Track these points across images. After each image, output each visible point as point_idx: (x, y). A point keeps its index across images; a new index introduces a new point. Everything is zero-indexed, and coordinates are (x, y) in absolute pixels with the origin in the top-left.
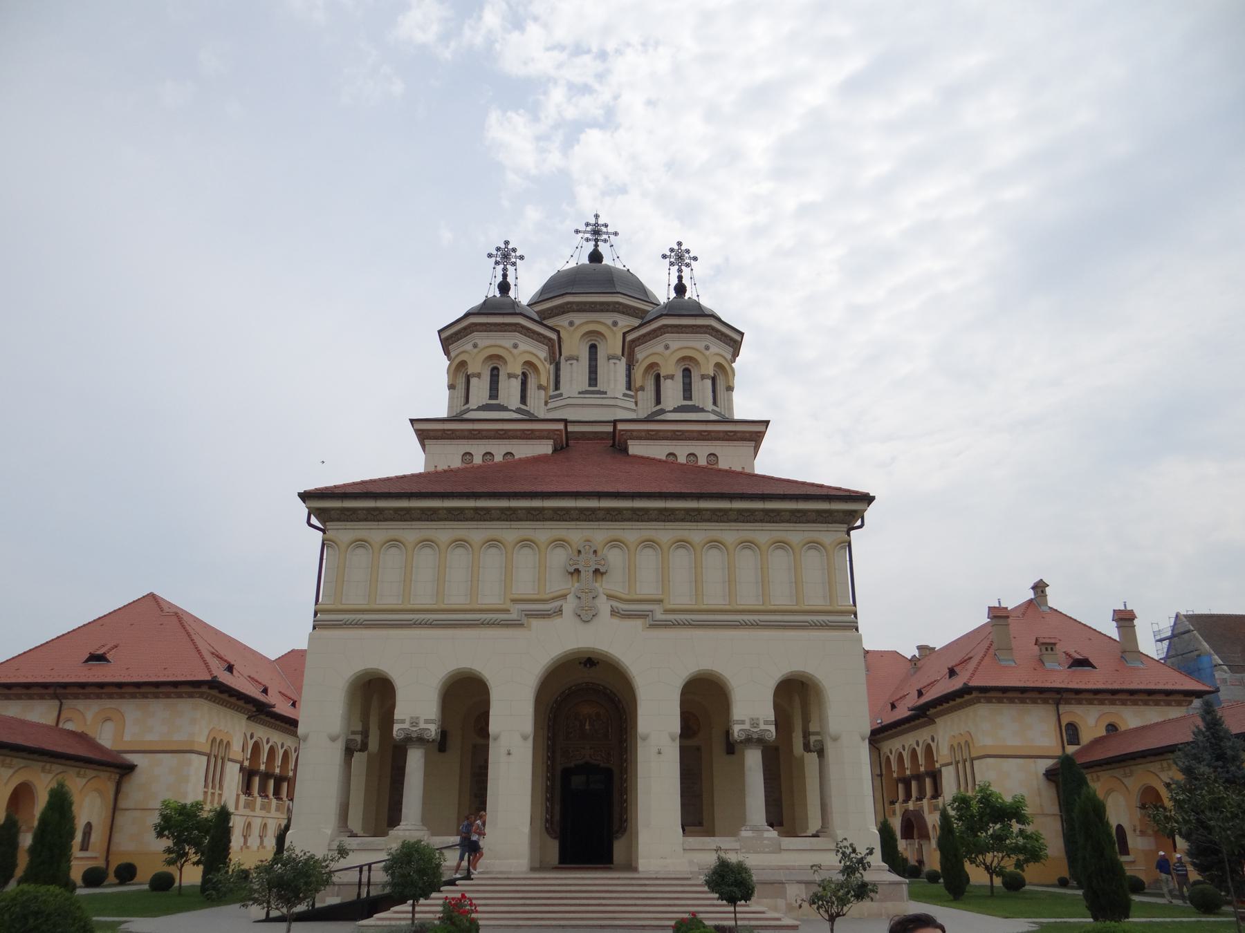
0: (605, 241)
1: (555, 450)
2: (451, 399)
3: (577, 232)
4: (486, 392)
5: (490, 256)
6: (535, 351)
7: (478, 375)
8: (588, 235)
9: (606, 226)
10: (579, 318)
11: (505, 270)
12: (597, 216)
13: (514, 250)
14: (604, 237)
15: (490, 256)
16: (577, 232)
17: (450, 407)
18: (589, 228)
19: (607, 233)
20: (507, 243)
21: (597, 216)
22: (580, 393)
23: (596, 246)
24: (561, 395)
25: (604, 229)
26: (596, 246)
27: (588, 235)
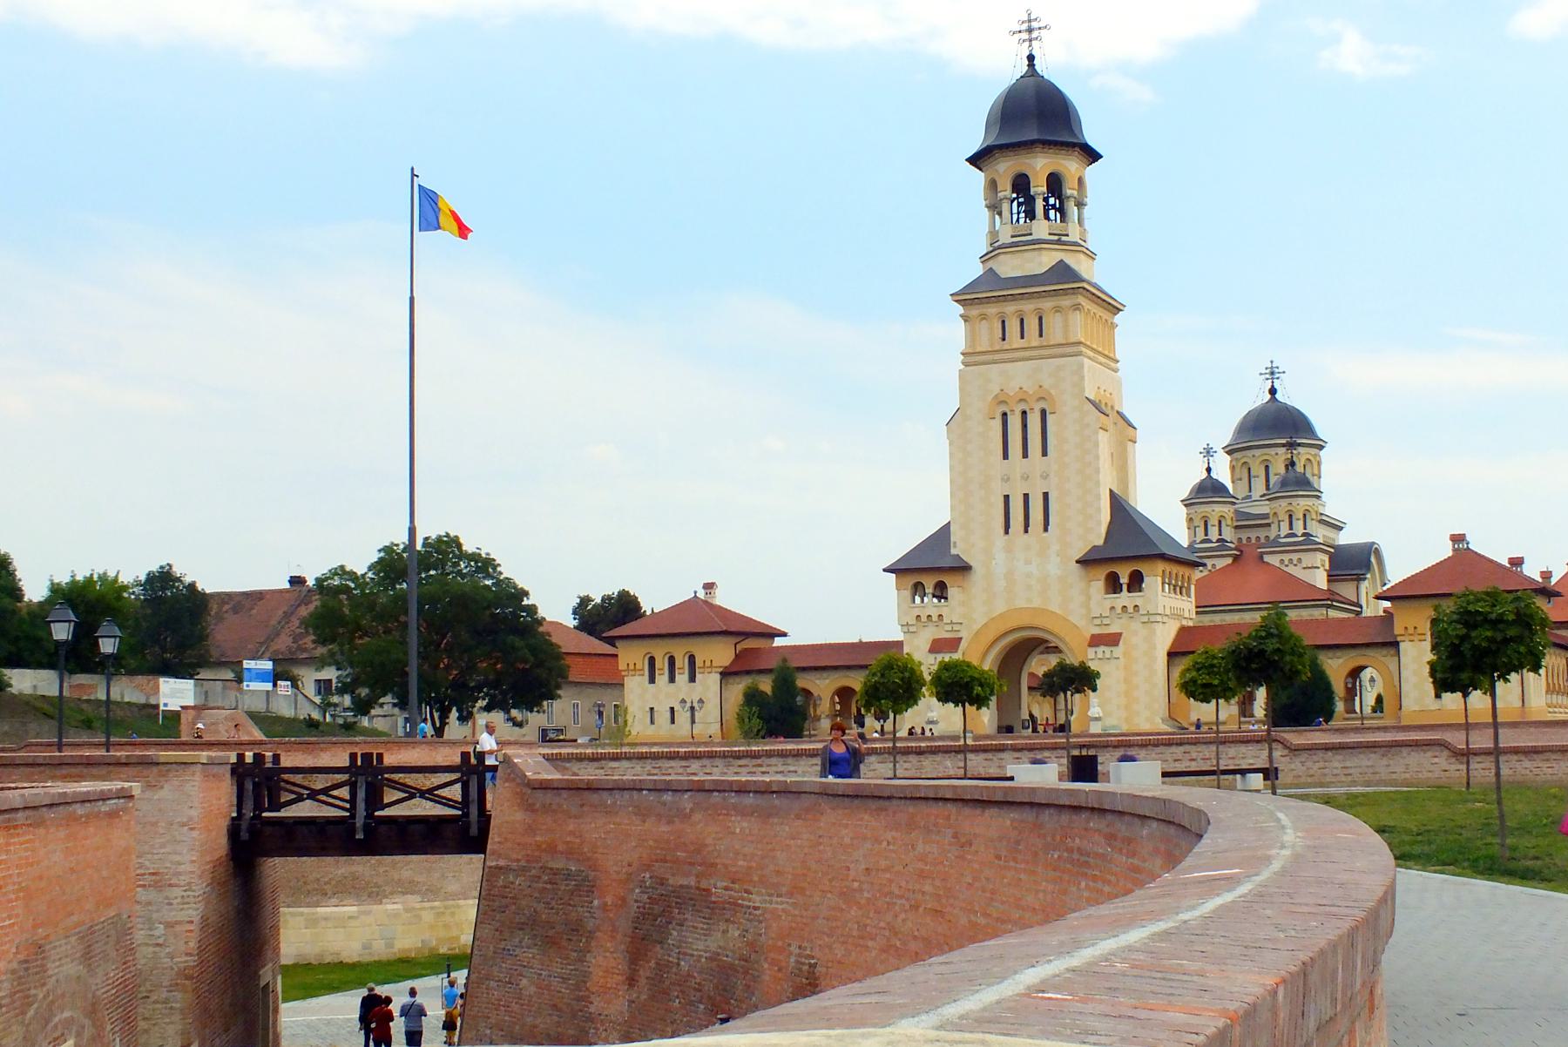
0: (1278, 378)
1: (1234, 561)
2: (1189, 534)
3: (1261, 374)
4: (1203, 534)
5: (1201, 453)
6: (1221, 509)
7: (1198, 526)
8: (1268, 376)
9: (1277, 368)
10: (1257, 452)
11: (1208, 460)
12: (1272, 362)
13: (1212, 448)
14: (1277, 375)
15: (1201, 453)
16: (1261, 374)
17: (1189, 538)
18: (1268, 371)
19: (1279, 373)
20: (1208, 445)
21: (1272, 362)
22: (1261, 496)
23: (1273, 382)
24: (1250, 497)
25: (1276, 370)
26: (1273, 382)
27: (1268, 376)
